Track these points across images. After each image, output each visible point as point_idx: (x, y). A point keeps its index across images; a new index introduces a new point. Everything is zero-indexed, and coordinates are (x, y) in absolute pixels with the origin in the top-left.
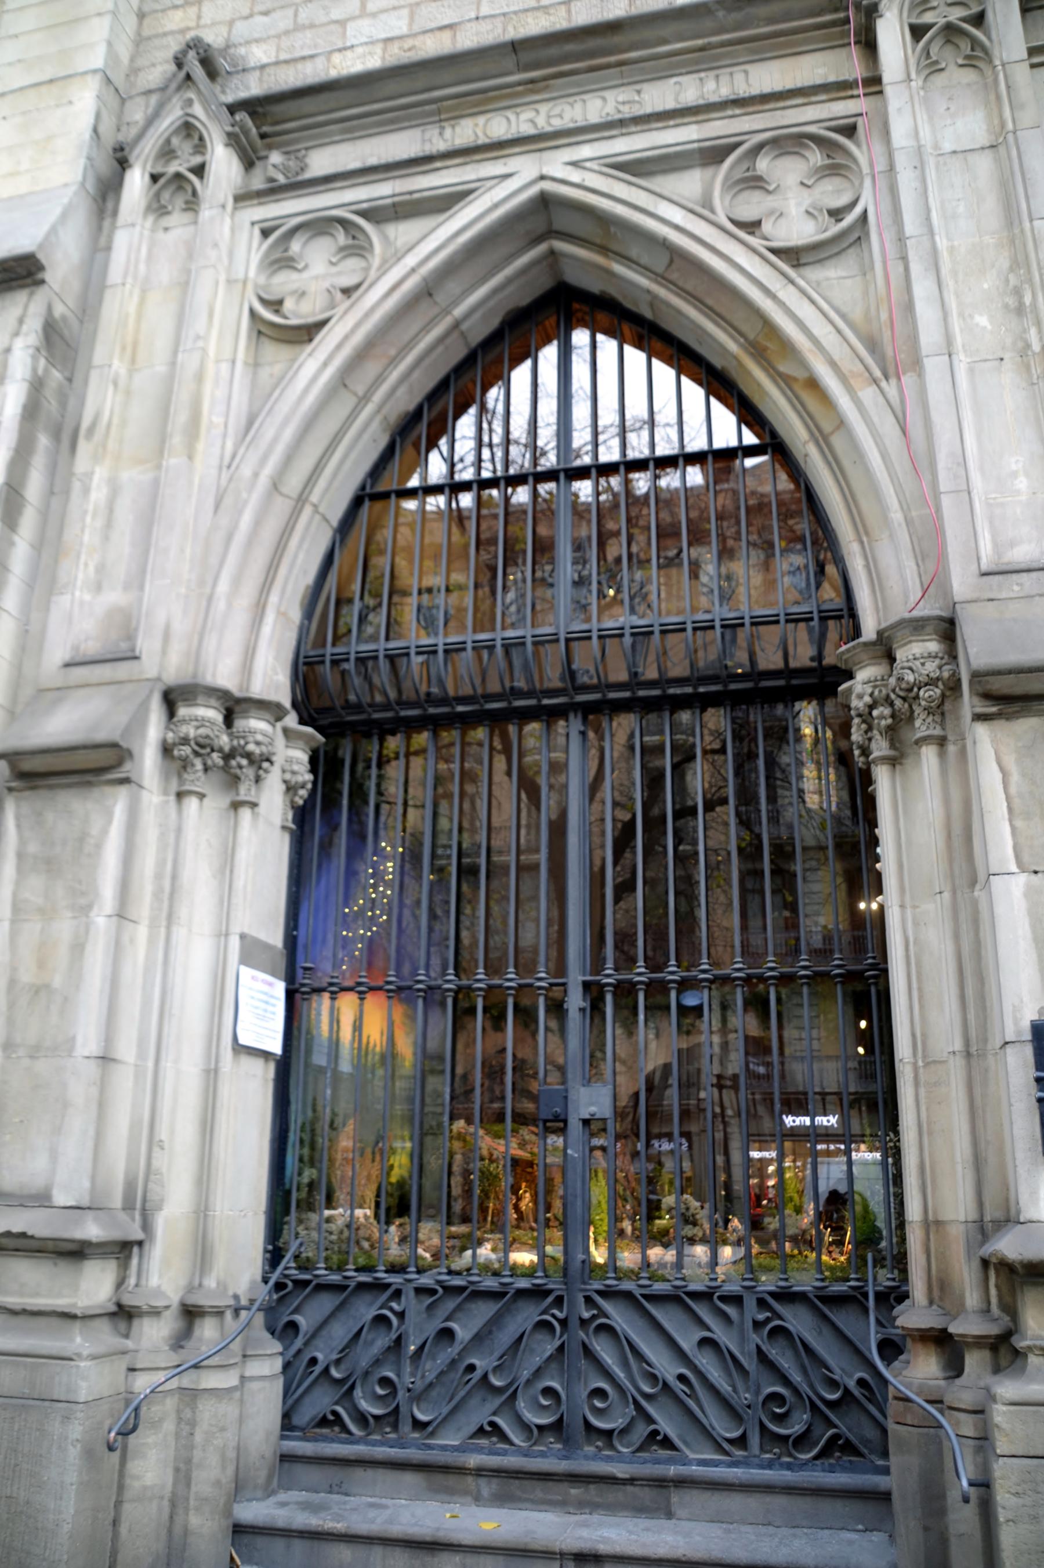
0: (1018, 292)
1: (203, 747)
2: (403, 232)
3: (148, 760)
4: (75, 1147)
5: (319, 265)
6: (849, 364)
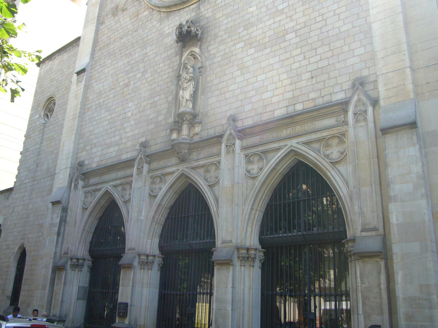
2: (97, 193)
4: (59, 310)
5: (89, 199)
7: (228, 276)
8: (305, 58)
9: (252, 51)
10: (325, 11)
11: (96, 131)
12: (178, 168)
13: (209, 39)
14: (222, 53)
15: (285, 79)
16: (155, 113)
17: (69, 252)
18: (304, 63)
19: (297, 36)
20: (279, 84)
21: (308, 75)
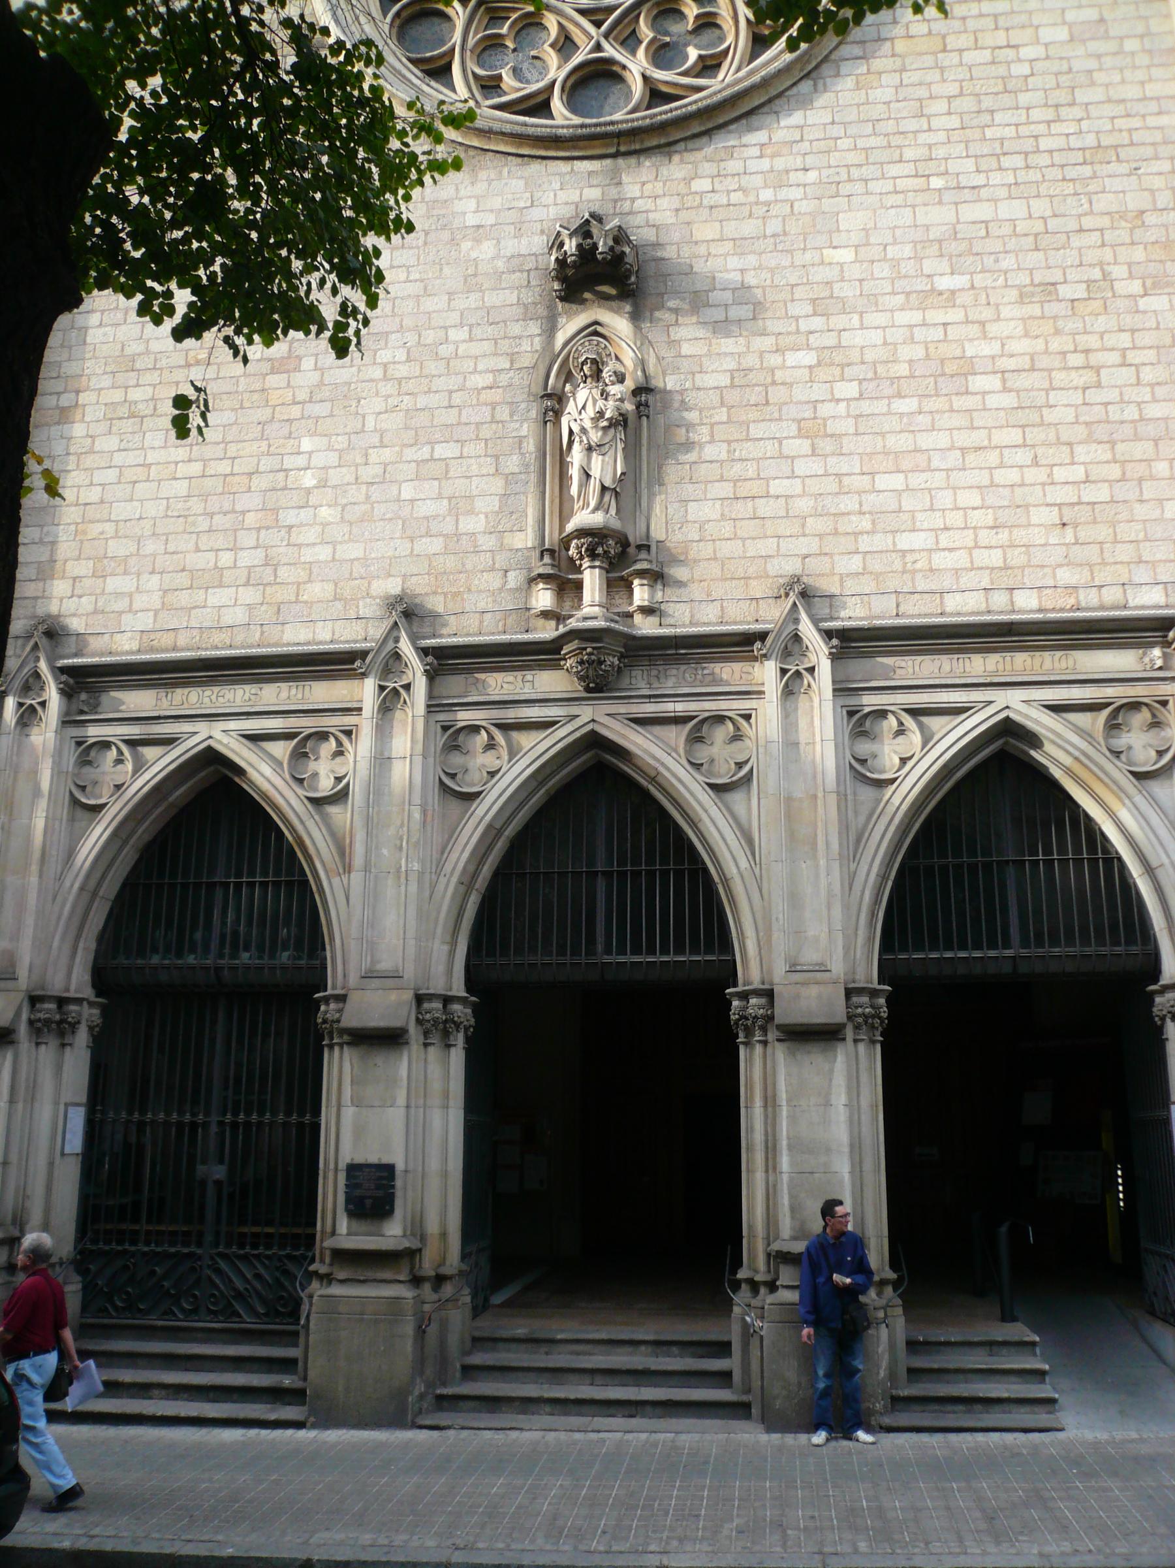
0: (401, 839)
1: (47, 1022)
3: (23, 1029)
6: (330, 865)
7: (831, 1071)
8: (1035, 463)
9: (849, 390)
10: (1093, 341)
11: (121, 511)
12: (574, 710)
15: (974, 509)
16: (445, 502)
17: (23, 973)
18: (1035, 475)
19: (1006, 389)
20: (955, 518)
21: (1053, 516)
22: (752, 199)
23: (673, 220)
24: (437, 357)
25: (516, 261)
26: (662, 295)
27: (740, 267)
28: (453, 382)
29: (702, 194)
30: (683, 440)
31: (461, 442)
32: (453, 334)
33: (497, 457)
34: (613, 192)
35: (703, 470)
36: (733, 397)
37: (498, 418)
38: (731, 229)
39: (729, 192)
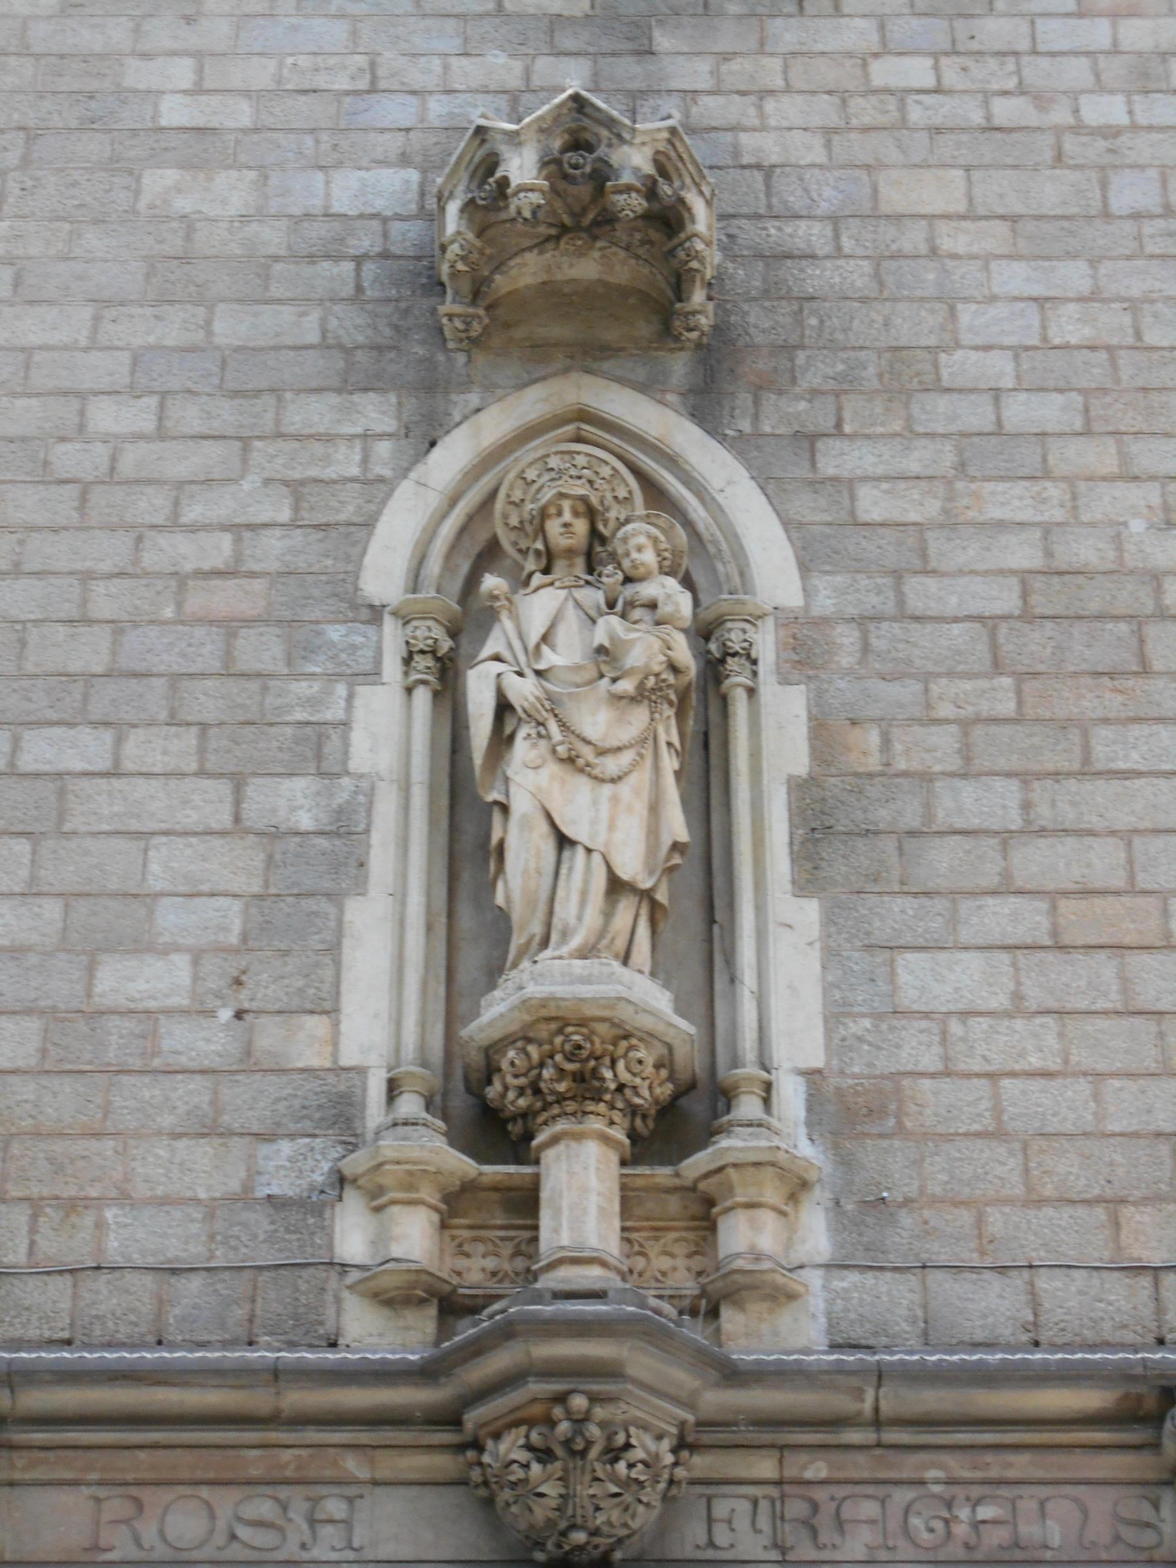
13: (817, 371)
14: (1022, 554)
22: (1060, 115)
23: (818, 155)
24: (46, 476)
25: (318, 231)
26: (788, 349)
27: (1038, 290)
28: (108, 551)
29: (902, 94)
30: (873, 763)
31: (118, 727)
32: (106, 417)
33: (238, 782)
34: (628, 71)
35: (942, 860)
36: (1036, 644)
37: (246, 661)
38: (999, 190)
39: (986, 96)
